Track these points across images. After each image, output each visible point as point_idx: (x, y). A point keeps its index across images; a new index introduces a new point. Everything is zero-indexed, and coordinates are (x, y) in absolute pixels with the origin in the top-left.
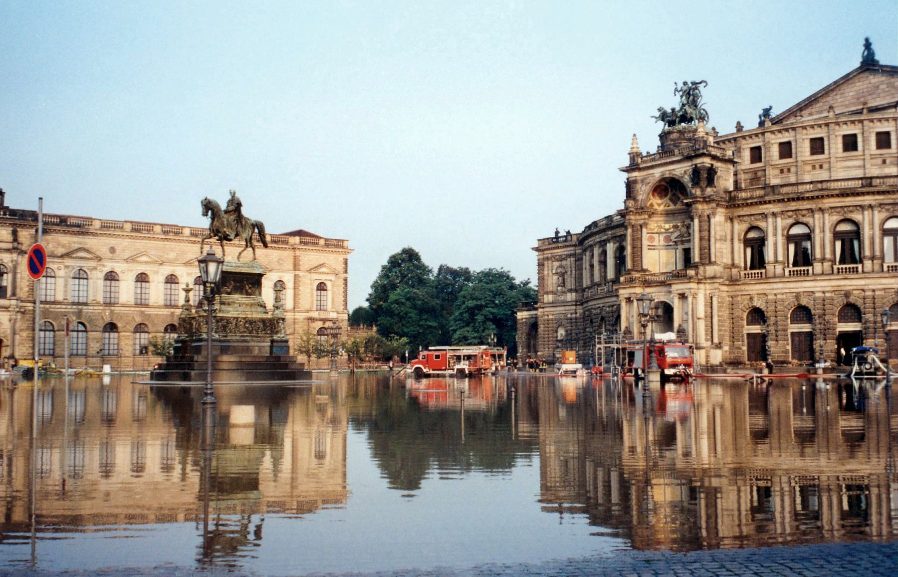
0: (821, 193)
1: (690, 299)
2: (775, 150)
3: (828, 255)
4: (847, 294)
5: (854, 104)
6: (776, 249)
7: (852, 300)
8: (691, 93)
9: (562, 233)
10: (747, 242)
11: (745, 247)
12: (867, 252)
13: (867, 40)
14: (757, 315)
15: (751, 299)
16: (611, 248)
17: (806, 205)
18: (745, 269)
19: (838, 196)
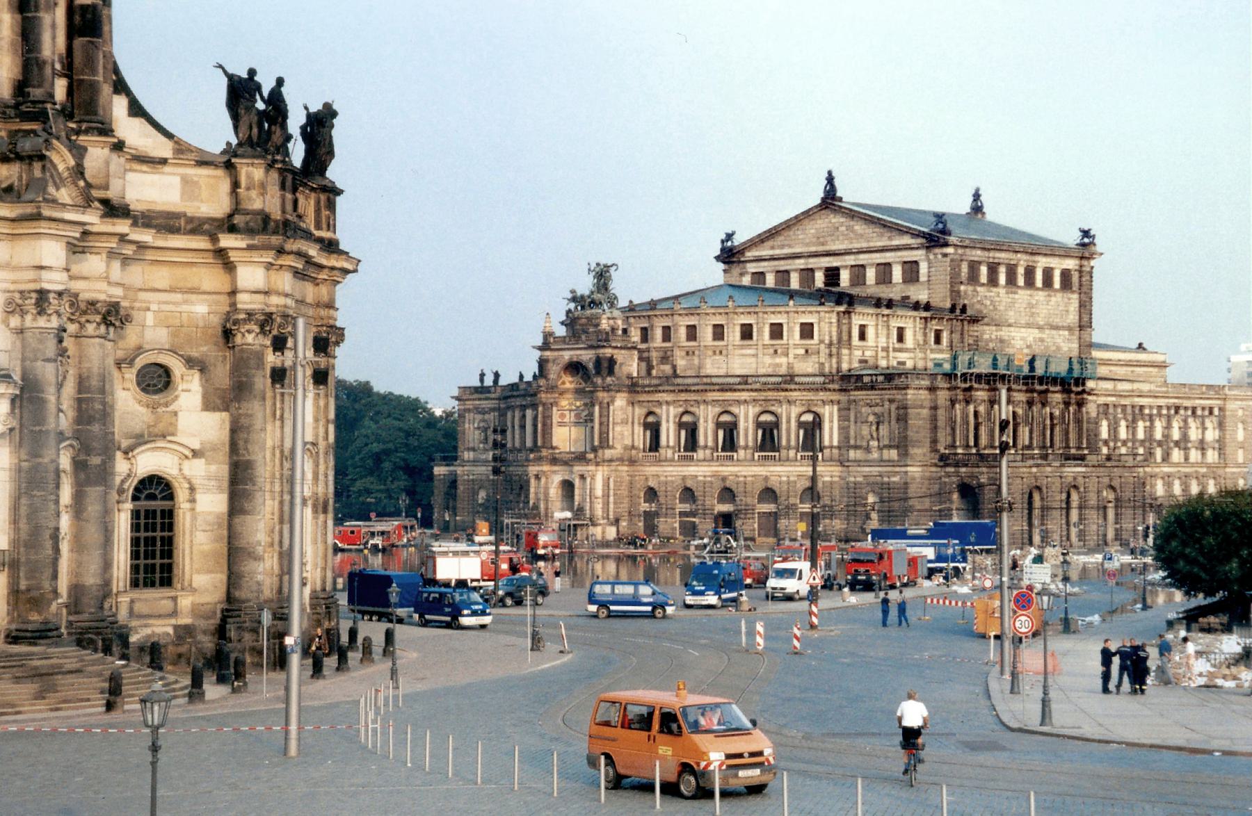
0: (708, 387)
1: (588, 480)
2: (683, 332)
3: (710, 444)
4: (724, 479)
5: (814, 245)
6: (669, 433)
7: (728, 484)
8: (602, 276)
10: (646, 426)
11: (645, 429)
12: (742, 443)
13: (830, 173)
14: (651, 494)
15: (647, 479)
17: (692, 397)
18: (644, 451)
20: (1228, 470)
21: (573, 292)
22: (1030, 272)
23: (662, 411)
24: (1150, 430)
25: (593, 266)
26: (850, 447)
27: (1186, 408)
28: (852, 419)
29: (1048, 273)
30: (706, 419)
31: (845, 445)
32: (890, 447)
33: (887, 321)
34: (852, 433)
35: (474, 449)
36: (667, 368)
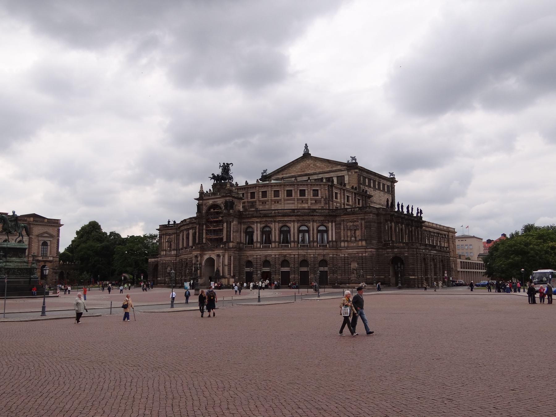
1: (222, 257)
5: (300, 172)
6: (257, 236)
8: (226, 168)
9: (172, 223)
10: (246, 233)
12: (292, 239)
13: (306, 145)
14: (249, 264)
16: (191, 232)
19: (281, 216)
20: (451, 258)
21: (213, 174)
22: (379, 183)
23: (254, 226)
24: (433, 241)
25: (222, 165)
26: (341, 241)
27: (441, 234)
28: (342, 228)
29: (384, 185)
30: (275, 228)
31: (338, 240)
32: (361, 240)
33: (344, 193)
34: (342, 234)
35: (165, 251)
36: (253, 209)
